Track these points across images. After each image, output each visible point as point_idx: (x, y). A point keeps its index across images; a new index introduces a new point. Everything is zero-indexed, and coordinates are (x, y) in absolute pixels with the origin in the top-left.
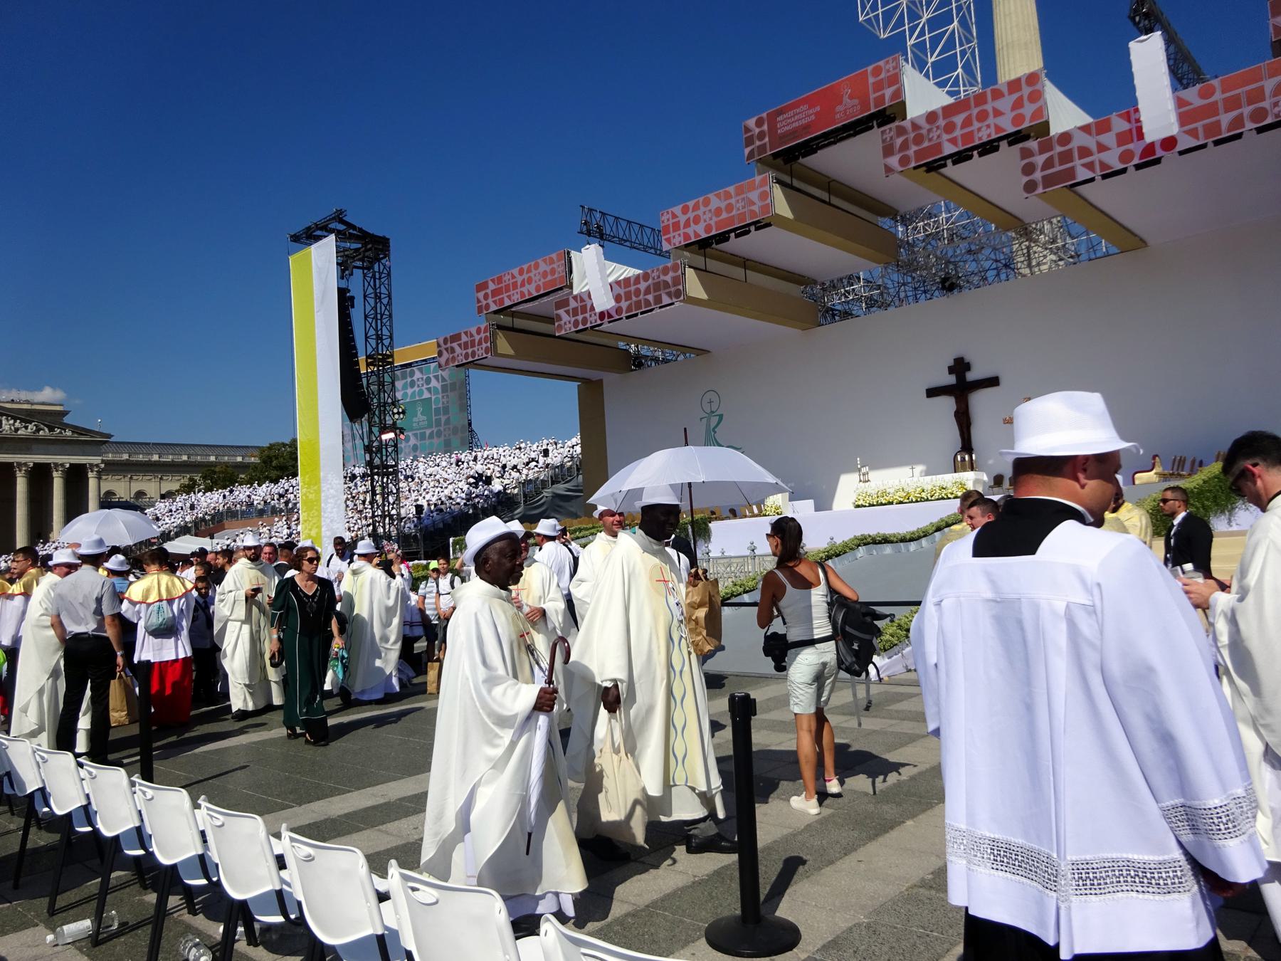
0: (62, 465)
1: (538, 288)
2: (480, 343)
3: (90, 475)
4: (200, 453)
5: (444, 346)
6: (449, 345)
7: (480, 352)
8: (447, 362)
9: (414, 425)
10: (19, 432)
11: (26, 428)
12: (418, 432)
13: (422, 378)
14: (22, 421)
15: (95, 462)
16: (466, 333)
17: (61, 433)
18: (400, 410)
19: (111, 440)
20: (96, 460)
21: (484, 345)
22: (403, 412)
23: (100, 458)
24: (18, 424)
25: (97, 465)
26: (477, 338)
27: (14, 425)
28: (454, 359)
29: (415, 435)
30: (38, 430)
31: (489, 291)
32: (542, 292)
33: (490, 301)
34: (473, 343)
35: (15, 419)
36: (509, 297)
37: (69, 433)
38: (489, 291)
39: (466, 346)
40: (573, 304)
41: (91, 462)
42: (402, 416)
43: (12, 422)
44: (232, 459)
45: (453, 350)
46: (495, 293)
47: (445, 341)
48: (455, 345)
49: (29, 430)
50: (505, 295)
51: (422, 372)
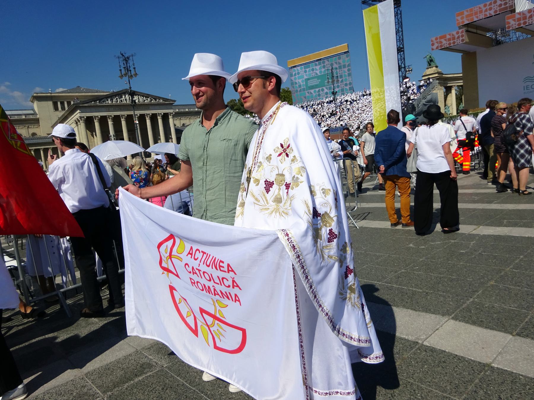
0: (161, 114)
1: (496, 11)
2: (458, 37)
3: (170, 117)
4: (182, 108)
5: (435, 41)
6: (438, 40)
7: (458, 42)
8: (437, 48)
9: (326, 84)
10: (145, 102)
11: (147, 100)
12: (328, 87)
13: (329, 64)
14: (146, 97)
15: (171, 112)
16: (450, 35)
17: (159, 101)
18: (410, 70)
19: (176, 104)
20: (171, 111)
21: (461, 39)
22: (411, 70)
23: (172, 110)
24: (144, 98)
25: (172, 113)
26: (456, 36)
27: (143, 99)
28: (441, 46)
29: (327, 88)
30: (151, 100)
31: (464, 16)
32: (498, 13)
33: (465, 20)
34: (454, 38)
35: (143, 96)
36: (477, 17)
37: (161, 101)
38: (464, 16)
39: (449, 40)
40: (517, 16)
41: (170, 112)
42: (410, 72)
43: (142, 98)
44: (194, 110)
45: (441, 42)
46: (467, 16)
47: (436, 39)
48: (443, 40)
49: (148, 101)
50: (474, 17)
51: (328, 61)
